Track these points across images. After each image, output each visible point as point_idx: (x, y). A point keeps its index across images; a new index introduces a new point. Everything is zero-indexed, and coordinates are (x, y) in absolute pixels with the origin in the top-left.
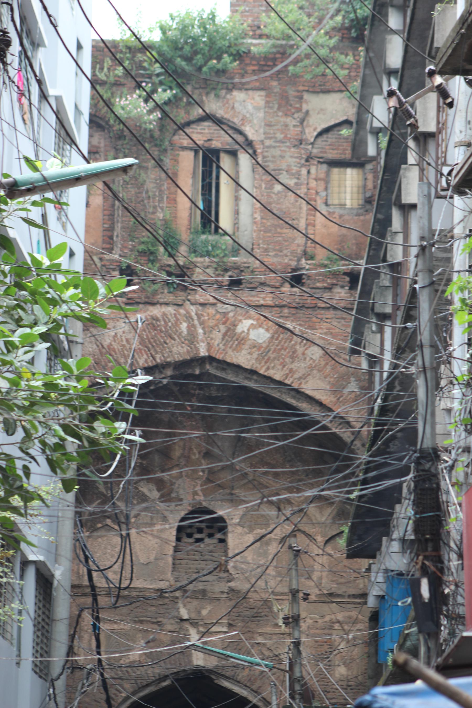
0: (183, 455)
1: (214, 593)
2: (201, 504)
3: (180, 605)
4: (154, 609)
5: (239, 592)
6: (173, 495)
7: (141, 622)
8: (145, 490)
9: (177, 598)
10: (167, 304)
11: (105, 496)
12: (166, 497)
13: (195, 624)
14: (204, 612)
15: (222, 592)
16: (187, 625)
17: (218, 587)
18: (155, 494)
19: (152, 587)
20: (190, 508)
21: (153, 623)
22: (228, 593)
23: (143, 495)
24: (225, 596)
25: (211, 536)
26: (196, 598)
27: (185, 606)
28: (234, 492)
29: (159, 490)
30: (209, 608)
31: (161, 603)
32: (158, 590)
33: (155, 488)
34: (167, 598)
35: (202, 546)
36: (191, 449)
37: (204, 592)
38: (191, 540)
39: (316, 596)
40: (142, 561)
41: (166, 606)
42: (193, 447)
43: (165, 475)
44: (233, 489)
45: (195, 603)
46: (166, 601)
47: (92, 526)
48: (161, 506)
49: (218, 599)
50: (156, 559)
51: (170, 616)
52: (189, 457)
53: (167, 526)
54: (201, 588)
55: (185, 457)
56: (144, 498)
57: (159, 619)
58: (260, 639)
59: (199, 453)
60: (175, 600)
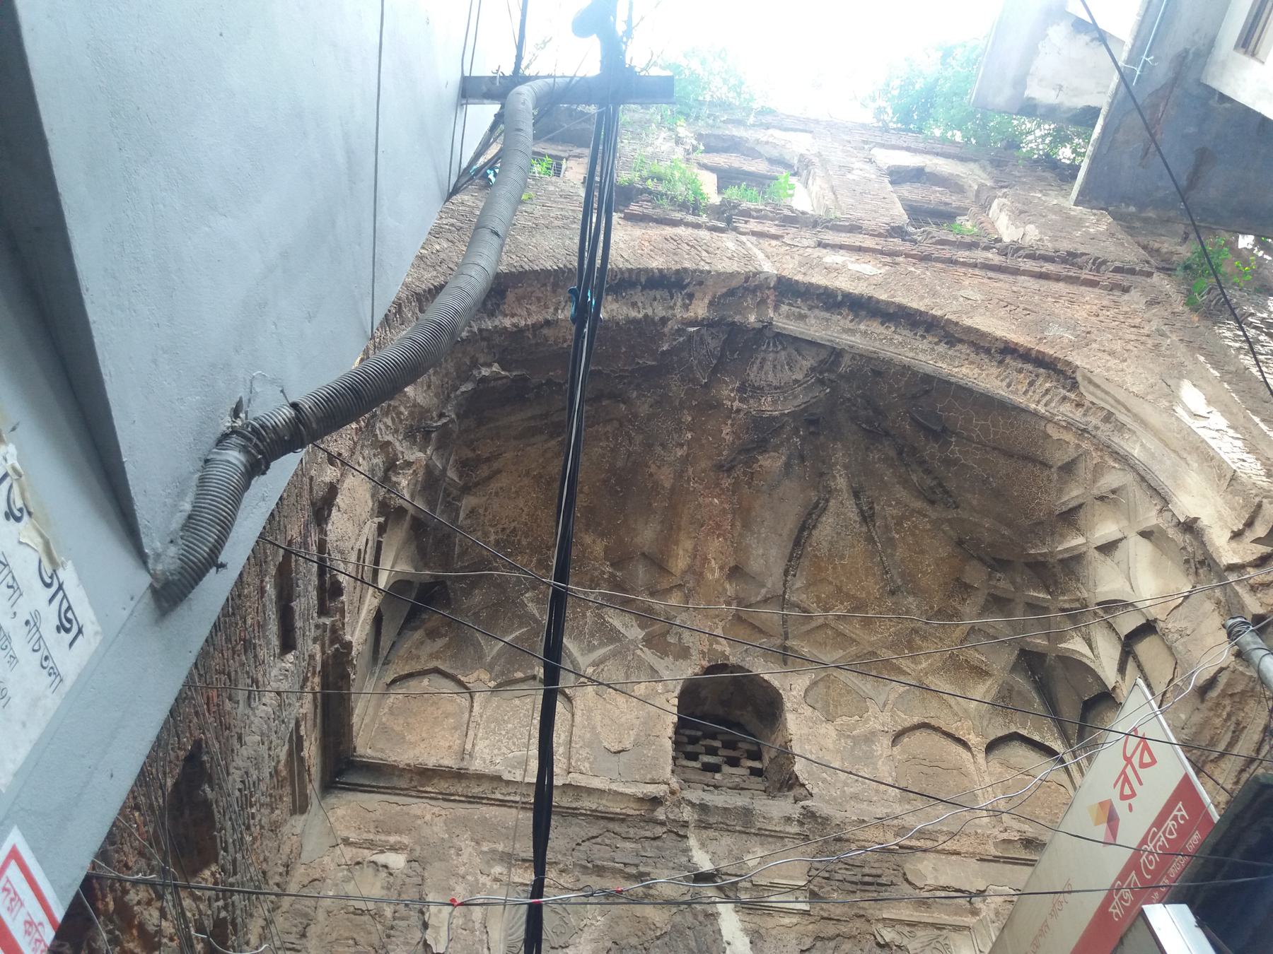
0: (690, 569)
1: (771, 819)
2: (727, 658)
3: (693, 842)
4: (629, 845)
5: (826, 820)
6: (672, 639)
7: (600, 871)
8: (617, 623)
9: (685, 825)
10: (697, 226)
11: (536, 621)
12: (656, 642)
13: (728, 893)
14: (751, 861)
15: (788, 819)
16: (708, 891)
17: (778, 809)
18: (634, 632)
19: (628, 791)
20: (706, 664)
21: (629, 877)
22: (801, 823)
23: (613, 629)
24: (794, 829)
25: (734, 762)
26: (729, 830)
27: (703, 845)
28: (788, 643)
29: (641, 627)
30: (760, 852)
31: (648, 834)
32: (641, 800)
33: (634, 623)
34: (662, 824)
35: (718, 776)
36: (705, 560)
37: (747, 813)
38: (693, 764)
39: (996, 845)
40: (605, 744)
41: (656, 843)
42: (710, 556)
43: (657, 604)
44: (786, 638)
45: (727, 840)
46: (659, 830)
47: (503, 674)
48: (648, 656)
49: (779, 837)
50: (636, 744)
51: (671, 864)
52: (701, 574)
53: (660, 687)
54: (739, 804)
55: (694, 573)
56: (613, 636)
57: (642, 869)
58: (888, 935)
59: (721, 568)
60: (678, 831)
